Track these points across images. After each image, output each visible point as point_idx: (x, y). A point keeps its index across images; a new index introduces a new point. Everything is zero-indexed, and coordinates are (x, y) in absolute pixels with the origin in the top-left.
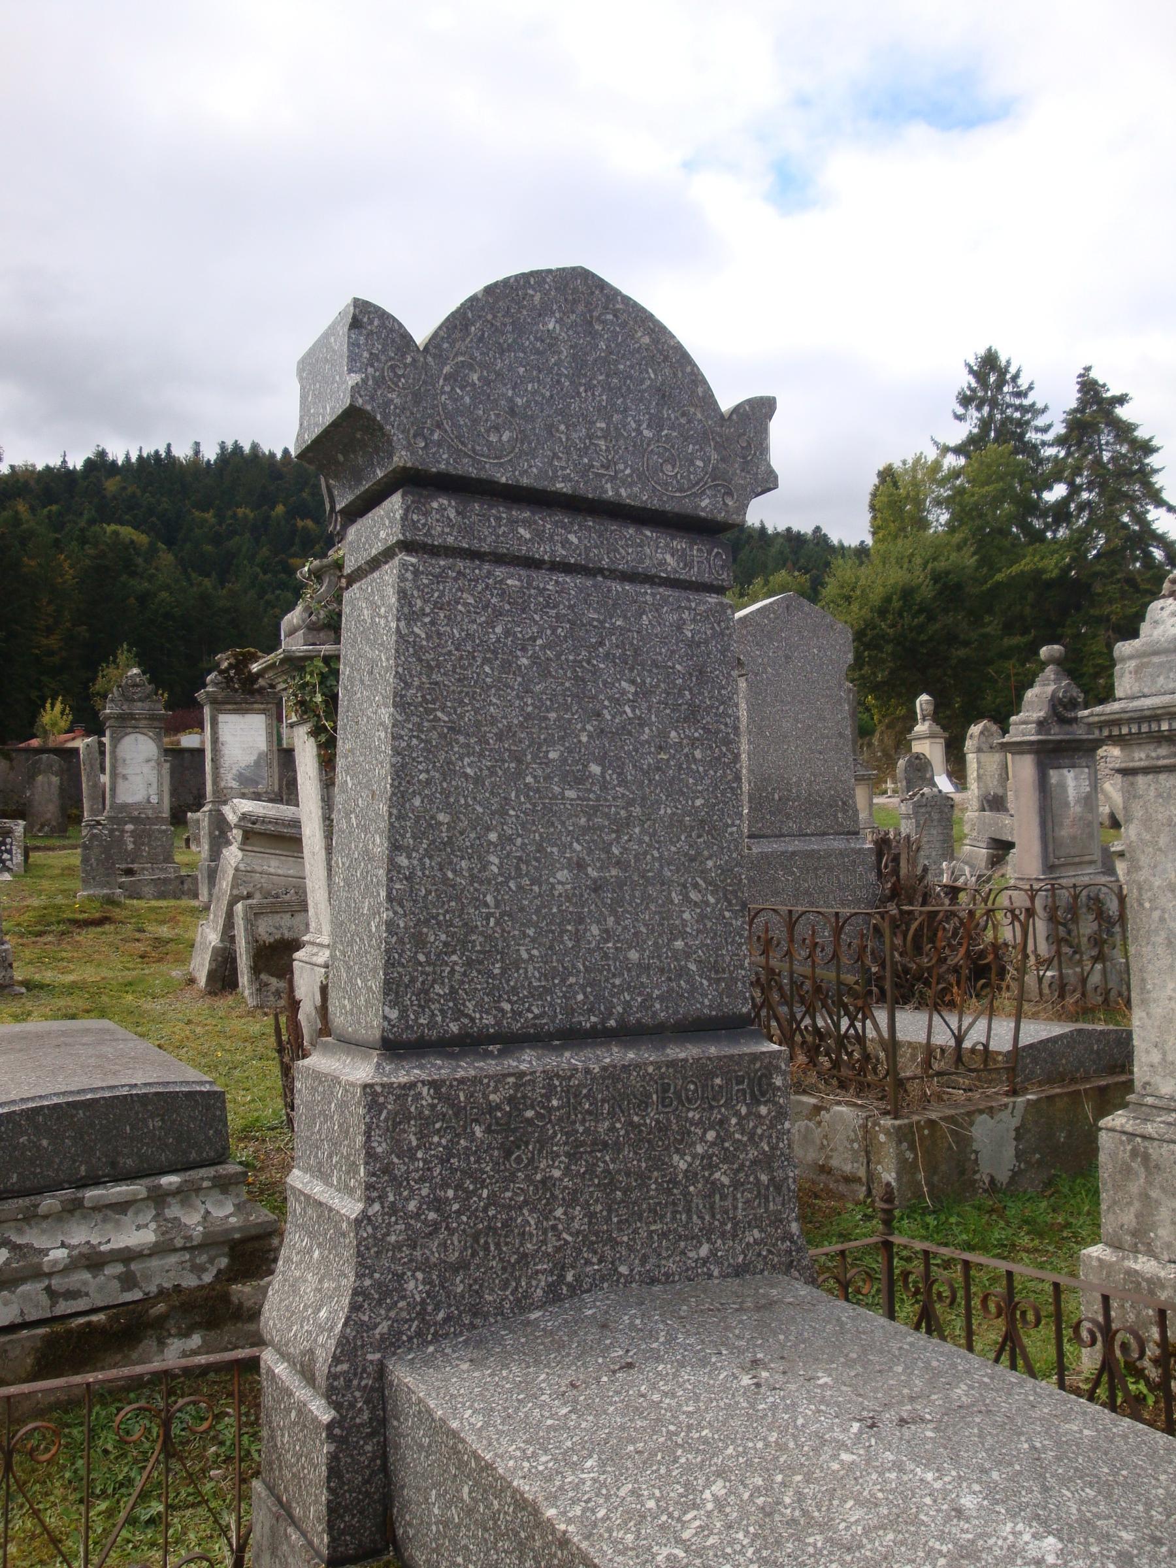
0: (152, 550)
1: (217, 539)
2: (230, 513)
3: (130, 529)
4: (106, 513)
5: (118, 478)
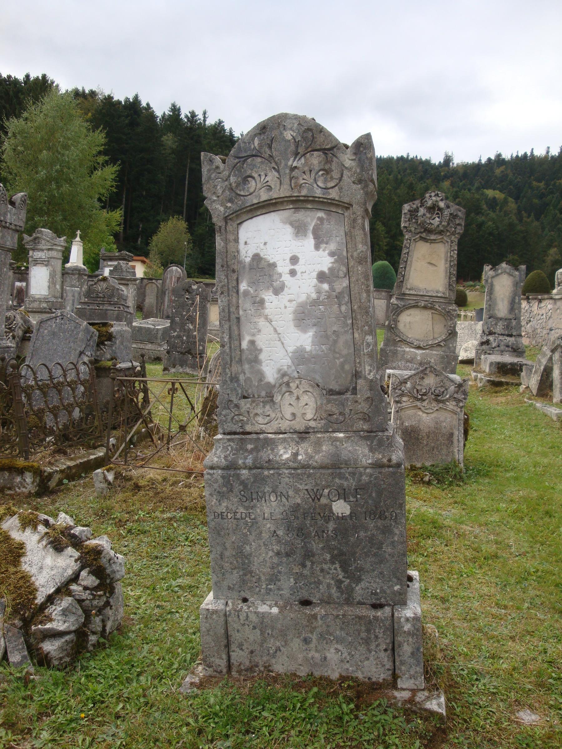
0: (505, 201)
1: (542, 196)
2: (553, 182)
3: (497, 192)
4: (488, 185)
5: (504, 167)
